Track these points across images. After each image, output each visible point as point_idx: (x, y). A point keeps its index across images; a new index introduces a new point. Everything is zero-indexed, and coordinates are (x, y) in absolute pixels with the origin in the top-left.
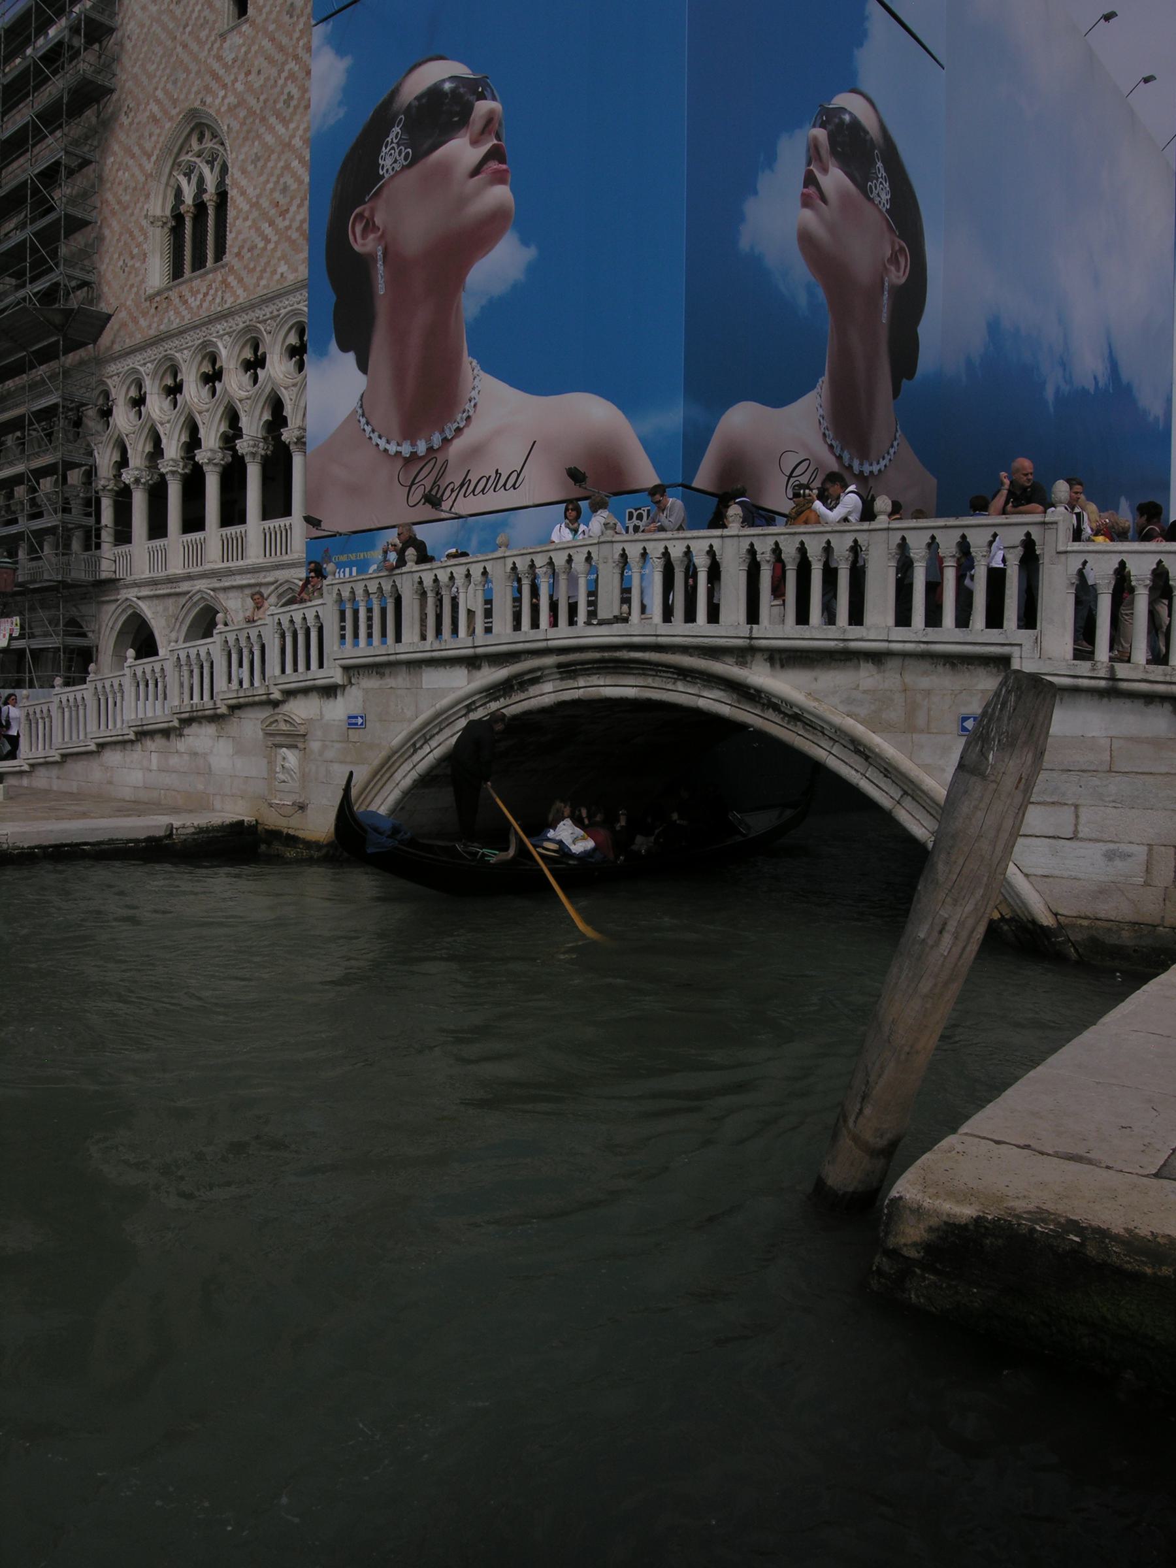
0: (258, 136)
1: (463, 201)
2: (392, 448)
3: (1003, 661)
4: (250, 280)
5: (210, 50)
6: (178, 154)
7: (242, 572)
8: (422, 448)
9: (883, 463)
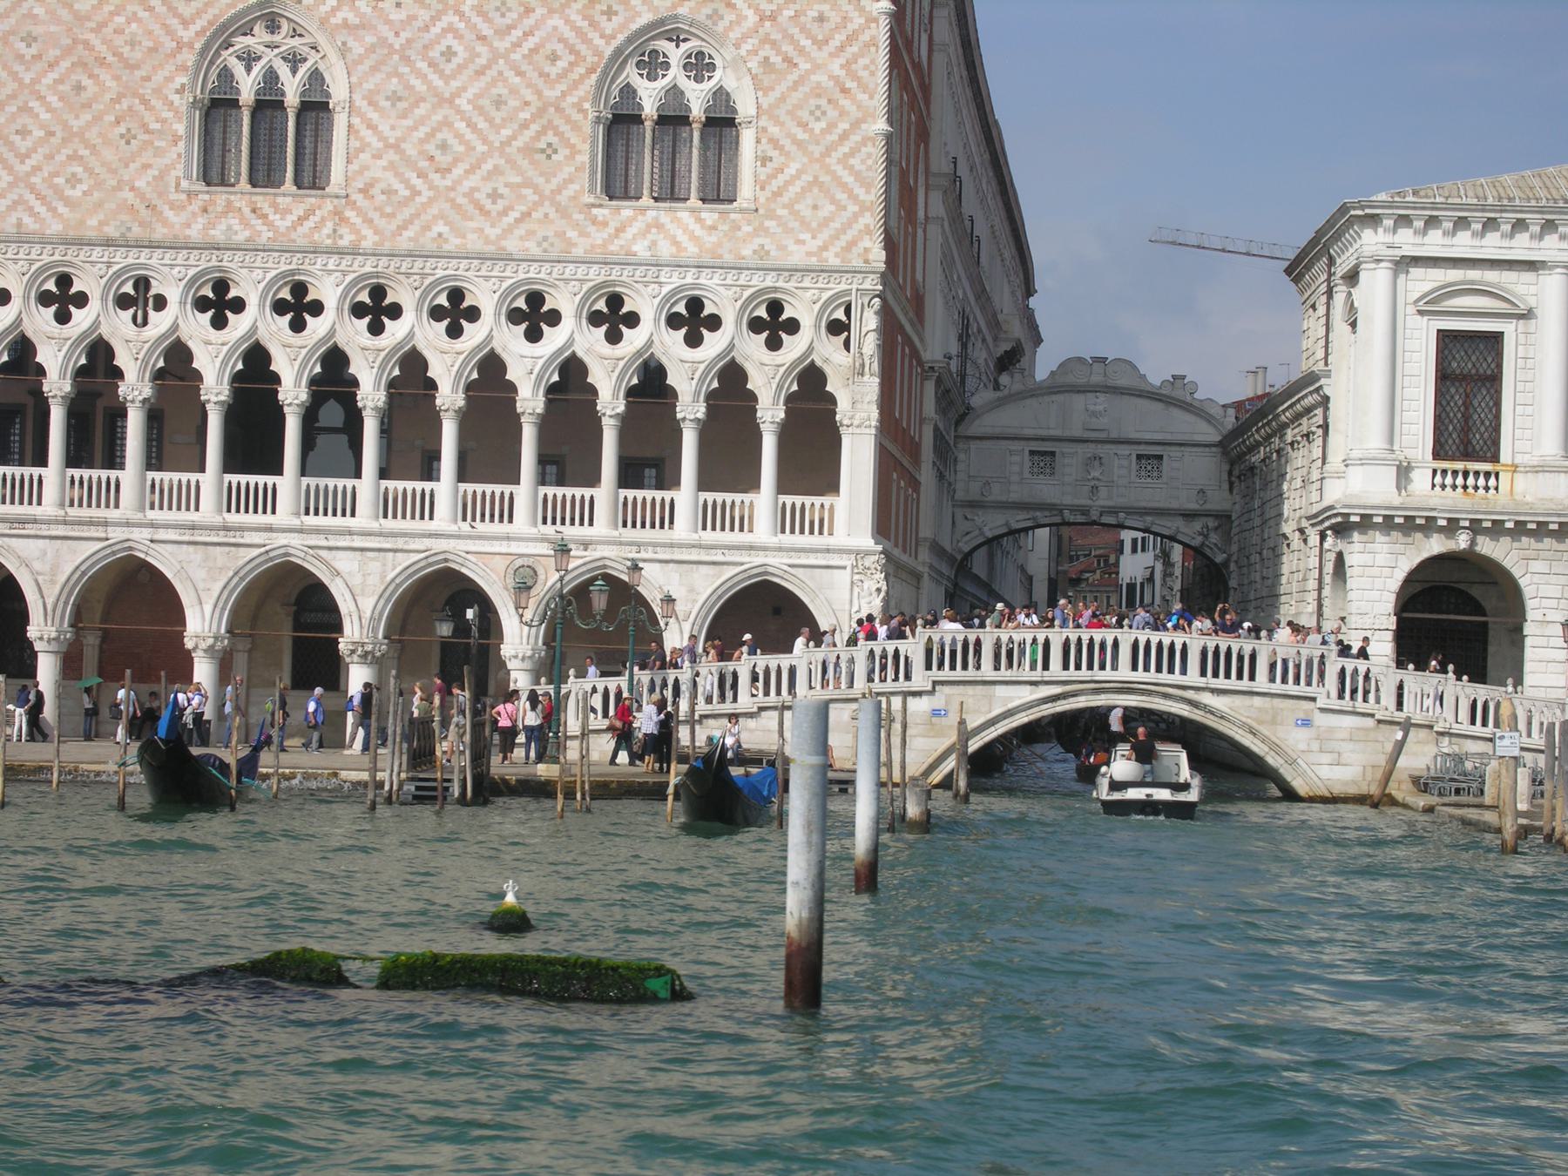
0: (400, 76)
3: (1314, 699)
4: (381, 222)
6: (232, 35)
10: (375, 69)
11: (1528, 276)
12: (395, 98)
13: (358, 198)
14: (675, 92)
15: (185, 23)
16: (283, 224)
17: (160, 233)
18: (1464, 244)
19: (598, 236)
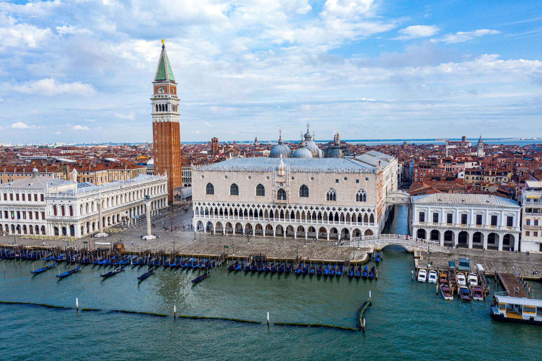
14: (361, 194)
17: (324, 204)
19: (356, 204)
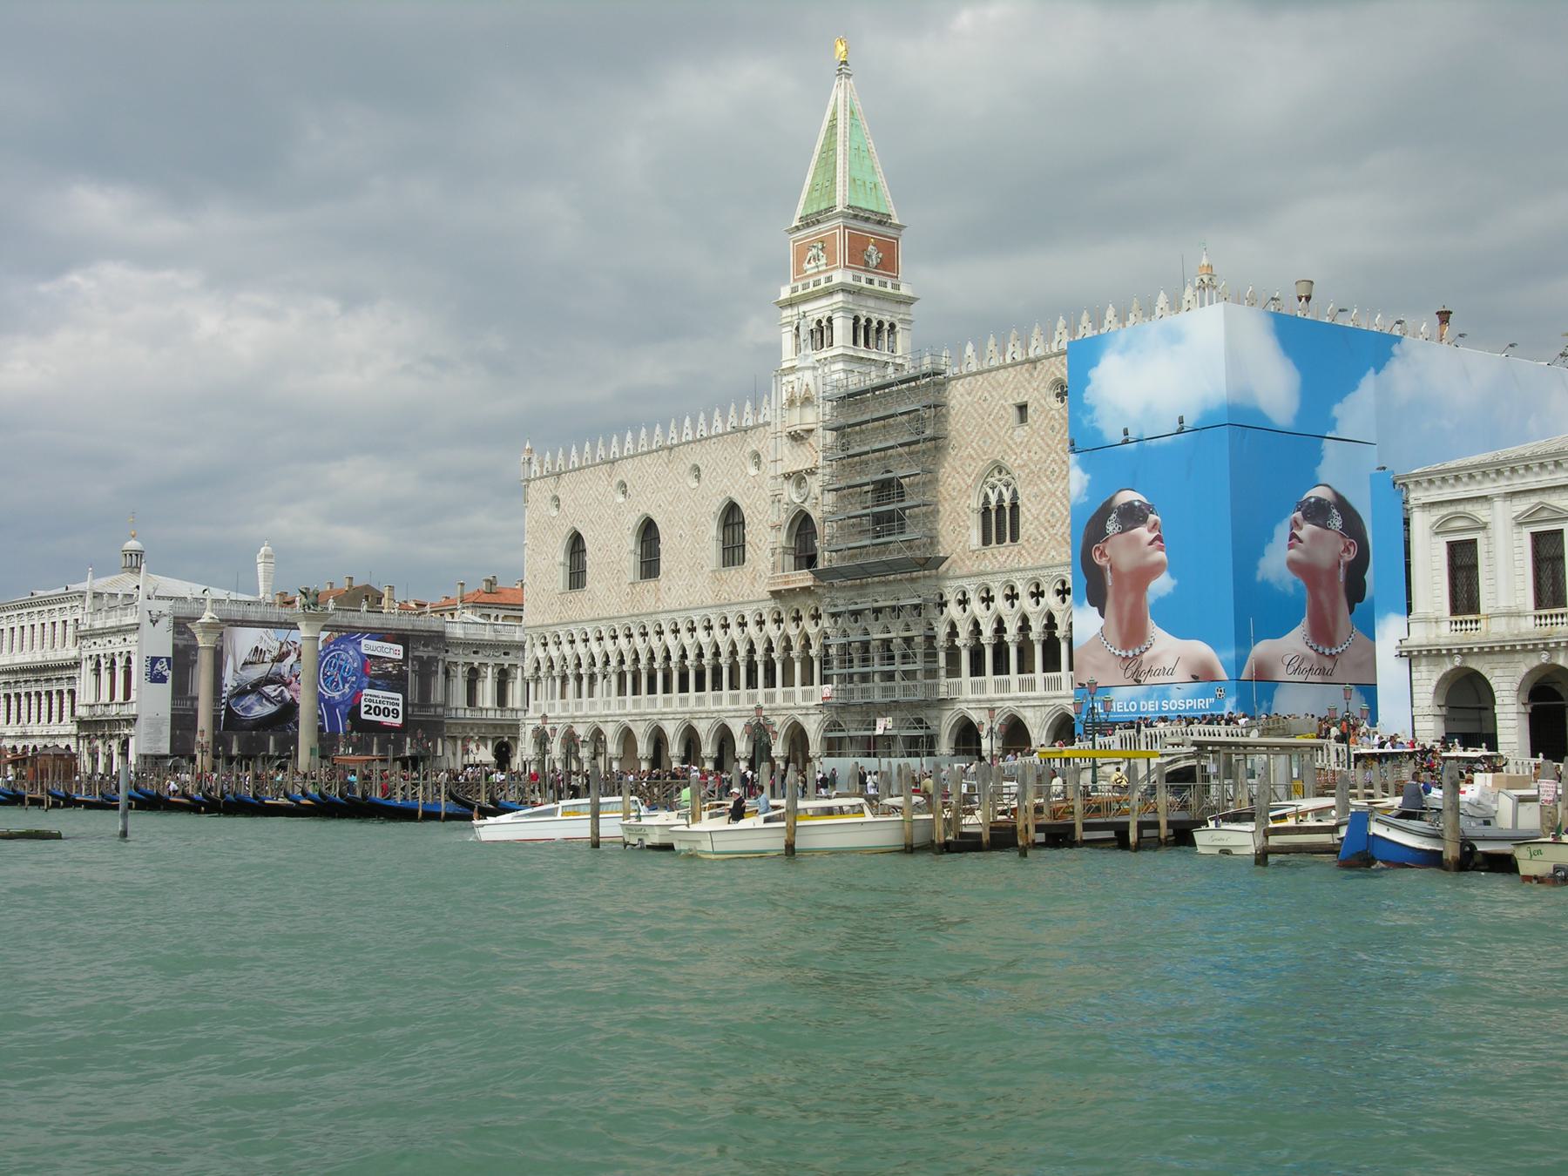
0: (1037, 485)
1: (1145, 555)
2: (1117, 652)
5: (1006, 432)
7: (1034, 699)
8: (1130, 654)
9: (1344, 646)
10: (1029, 484)
11: (1486, 506)
12: (1036, 496)
13: (1025, 544)
15: (969, 476)
16: (1002, 560)
18: (1447, 493)
